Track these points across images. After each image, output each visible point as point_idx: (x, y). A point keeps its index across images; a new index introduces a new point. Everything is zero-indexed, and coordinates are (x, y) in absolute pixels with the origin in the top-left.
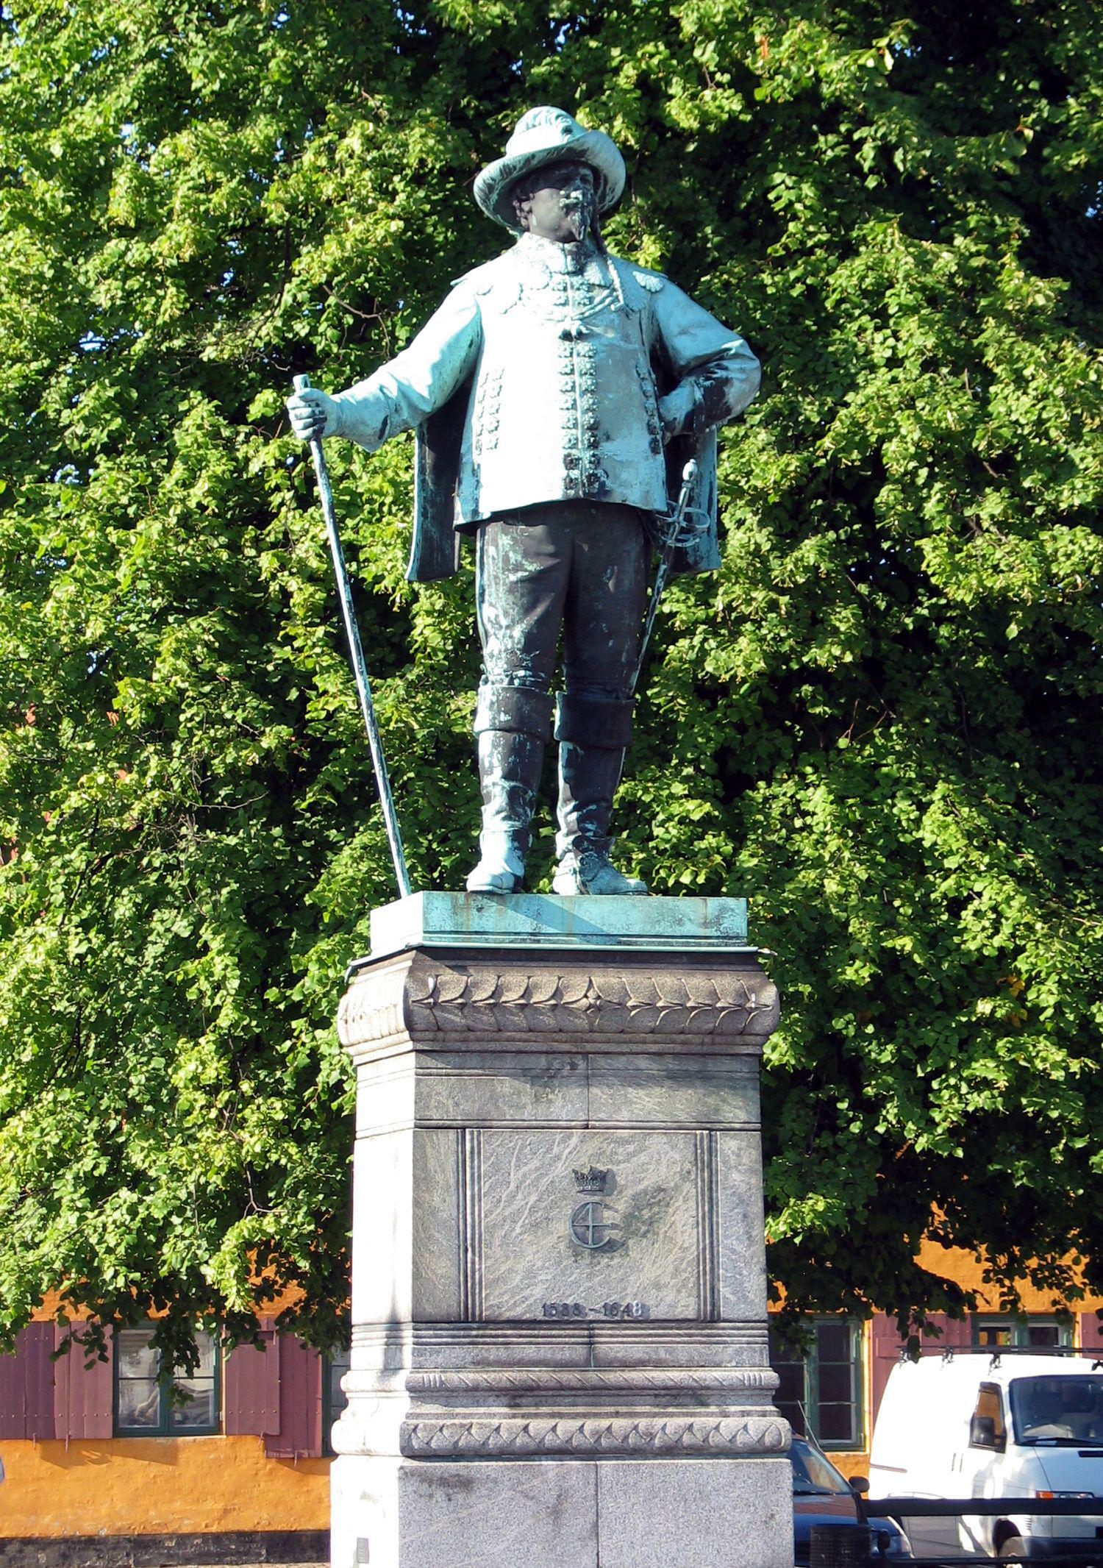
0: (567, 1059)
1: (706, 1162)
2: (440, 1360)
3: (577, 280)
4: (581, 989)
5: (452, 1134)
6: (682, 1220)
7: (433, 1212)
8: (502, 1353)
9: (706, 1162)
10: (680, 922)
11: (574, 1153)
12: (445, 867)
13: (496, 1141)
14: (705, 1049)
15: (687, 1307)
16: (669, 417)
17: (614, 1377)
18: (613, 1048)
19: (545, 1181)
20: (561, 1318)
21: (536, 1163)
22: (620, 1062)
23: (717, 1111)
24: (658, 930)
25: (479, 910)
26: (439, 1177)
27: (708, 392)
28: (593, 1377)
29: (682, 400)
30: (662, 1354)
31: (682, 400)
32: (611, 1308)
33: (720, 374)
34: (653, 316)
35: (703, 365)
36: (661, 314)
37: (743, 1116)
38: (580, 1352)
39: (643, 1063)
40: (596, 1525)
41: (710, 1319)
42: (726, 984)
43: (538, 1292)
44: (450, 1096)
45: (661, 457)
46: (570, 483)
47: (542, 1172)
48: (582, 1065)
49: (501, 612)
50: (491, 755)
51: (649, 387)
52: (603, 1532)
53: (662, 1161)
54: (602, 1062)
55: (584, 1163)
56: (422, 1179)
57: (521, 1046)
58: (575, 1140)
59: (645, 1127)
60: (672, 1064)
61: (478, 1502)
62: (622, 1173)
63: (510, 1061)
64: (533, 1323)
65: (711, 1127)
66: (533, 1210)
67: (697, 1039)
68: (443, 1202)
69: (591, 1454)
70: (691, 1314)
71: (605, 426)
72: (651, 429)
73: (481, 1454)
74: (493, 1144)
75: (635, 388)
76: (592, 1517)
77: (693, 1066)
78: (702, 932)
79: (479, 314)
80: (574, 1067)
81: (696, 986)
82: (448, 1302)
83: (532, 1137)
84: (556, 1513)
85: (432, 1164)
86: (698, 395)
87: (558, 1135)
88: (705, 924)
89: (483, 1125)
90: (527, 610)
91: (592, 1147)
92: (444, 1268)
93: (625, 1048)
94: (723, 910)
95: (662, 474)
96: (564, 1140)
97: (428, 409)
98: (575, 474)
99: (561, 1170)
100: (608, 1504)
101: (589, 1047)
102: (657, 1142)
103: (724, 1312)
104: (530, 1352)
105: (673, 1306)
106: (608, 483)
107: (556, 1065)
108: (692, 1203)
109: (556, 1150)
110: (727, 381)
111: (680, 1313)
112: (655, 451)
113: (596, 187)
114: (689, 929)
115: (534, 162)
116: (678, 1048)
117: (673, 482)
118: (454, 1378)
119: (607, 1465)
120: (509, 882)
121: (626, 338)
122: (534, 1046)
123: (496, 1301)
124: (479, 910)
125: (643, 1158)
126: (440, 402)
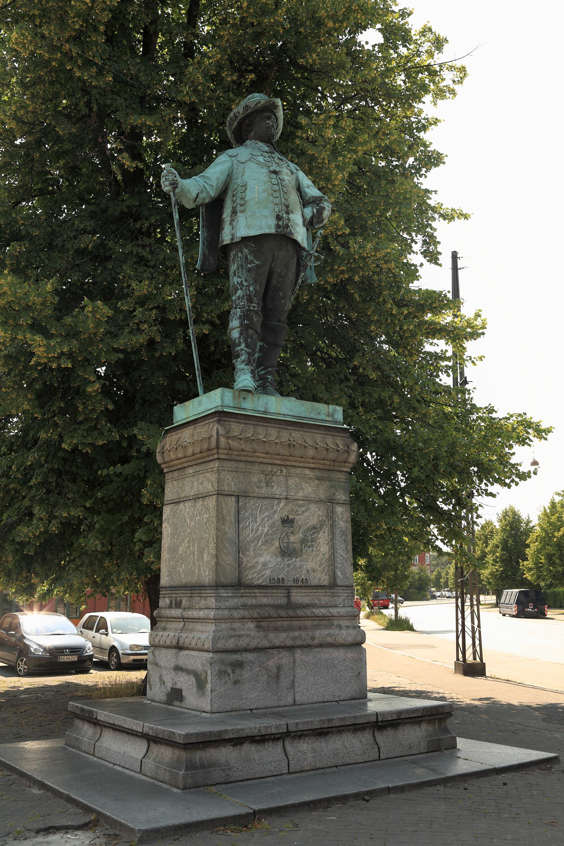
0: (279, 467)
1: (331, 515)
2: (228, 604)
5: (233, 499)
7: (226, 533)
8: (254, 601)
9: (331, 515)
11: (281, 510)
14: (331, 468)
15: (325, 580)
17: (300, 612)
18: (297, 464)
20: (275, 585)
21: (267, 514)
22: (299, 471)
23: (334, 495)
24: (313, 416)
25: (244, 399)
26: (228, 518)
27: (317, 210)
28: (291, 613)
30: (316, 602)
32: (296, 580)
37: (344, 498)
38: (284, 601)
39: (307, 472)
40: (293, 682)
41: (333, 585)
43: (268, 572)
44: (233, 481)
46: (278, 226)
47: (269, 517)
48: (285, 471)
49: (243, 279)
50: (239, 338)
52: (297, 684)
53: (312, 515)
54: (292, 470)
55: (284, 514)
57: (262, 460)
58: (282, 504)
59: (308, 500)
60: (318, 473)
61: (246, 674)
62: (300, 519)
63: (257, 468)
64: (266, 587)
65: (331, 501)
66: (267, 534)
67: (328, 463)
68: (229, 530)
69: (291, 648)
70: (326, 583)
73: (247, 650)
76: (292, 678)
77: (326, 475)
78: (328, 419)
80: (282, 471)
82: (230, 576)
83: (266, 502)
84: (278, 676)
85: (225, 512)
88: (328, 416)
90: (255, 280)
91: (289, 508)
92: (229, 560)
93: (301, 465)
94: (335, 410)
96: (278, 504)
98: (281, 223)
99: (277, 517)
100: (300, 673)
101: (288, 463)
103: (339, 582)
104: (265, 601)
105: (320, 580)
107: (275, 470)
108: (326, 534)
109: (275, 508)
115: (259, 105)
116: (321, 467)
118: (236, 614)
119: (298, 652)
122: (266, 461)
123: (252, 576)
124: (244, 399)
125: (307, 514)
126: (216, 195)
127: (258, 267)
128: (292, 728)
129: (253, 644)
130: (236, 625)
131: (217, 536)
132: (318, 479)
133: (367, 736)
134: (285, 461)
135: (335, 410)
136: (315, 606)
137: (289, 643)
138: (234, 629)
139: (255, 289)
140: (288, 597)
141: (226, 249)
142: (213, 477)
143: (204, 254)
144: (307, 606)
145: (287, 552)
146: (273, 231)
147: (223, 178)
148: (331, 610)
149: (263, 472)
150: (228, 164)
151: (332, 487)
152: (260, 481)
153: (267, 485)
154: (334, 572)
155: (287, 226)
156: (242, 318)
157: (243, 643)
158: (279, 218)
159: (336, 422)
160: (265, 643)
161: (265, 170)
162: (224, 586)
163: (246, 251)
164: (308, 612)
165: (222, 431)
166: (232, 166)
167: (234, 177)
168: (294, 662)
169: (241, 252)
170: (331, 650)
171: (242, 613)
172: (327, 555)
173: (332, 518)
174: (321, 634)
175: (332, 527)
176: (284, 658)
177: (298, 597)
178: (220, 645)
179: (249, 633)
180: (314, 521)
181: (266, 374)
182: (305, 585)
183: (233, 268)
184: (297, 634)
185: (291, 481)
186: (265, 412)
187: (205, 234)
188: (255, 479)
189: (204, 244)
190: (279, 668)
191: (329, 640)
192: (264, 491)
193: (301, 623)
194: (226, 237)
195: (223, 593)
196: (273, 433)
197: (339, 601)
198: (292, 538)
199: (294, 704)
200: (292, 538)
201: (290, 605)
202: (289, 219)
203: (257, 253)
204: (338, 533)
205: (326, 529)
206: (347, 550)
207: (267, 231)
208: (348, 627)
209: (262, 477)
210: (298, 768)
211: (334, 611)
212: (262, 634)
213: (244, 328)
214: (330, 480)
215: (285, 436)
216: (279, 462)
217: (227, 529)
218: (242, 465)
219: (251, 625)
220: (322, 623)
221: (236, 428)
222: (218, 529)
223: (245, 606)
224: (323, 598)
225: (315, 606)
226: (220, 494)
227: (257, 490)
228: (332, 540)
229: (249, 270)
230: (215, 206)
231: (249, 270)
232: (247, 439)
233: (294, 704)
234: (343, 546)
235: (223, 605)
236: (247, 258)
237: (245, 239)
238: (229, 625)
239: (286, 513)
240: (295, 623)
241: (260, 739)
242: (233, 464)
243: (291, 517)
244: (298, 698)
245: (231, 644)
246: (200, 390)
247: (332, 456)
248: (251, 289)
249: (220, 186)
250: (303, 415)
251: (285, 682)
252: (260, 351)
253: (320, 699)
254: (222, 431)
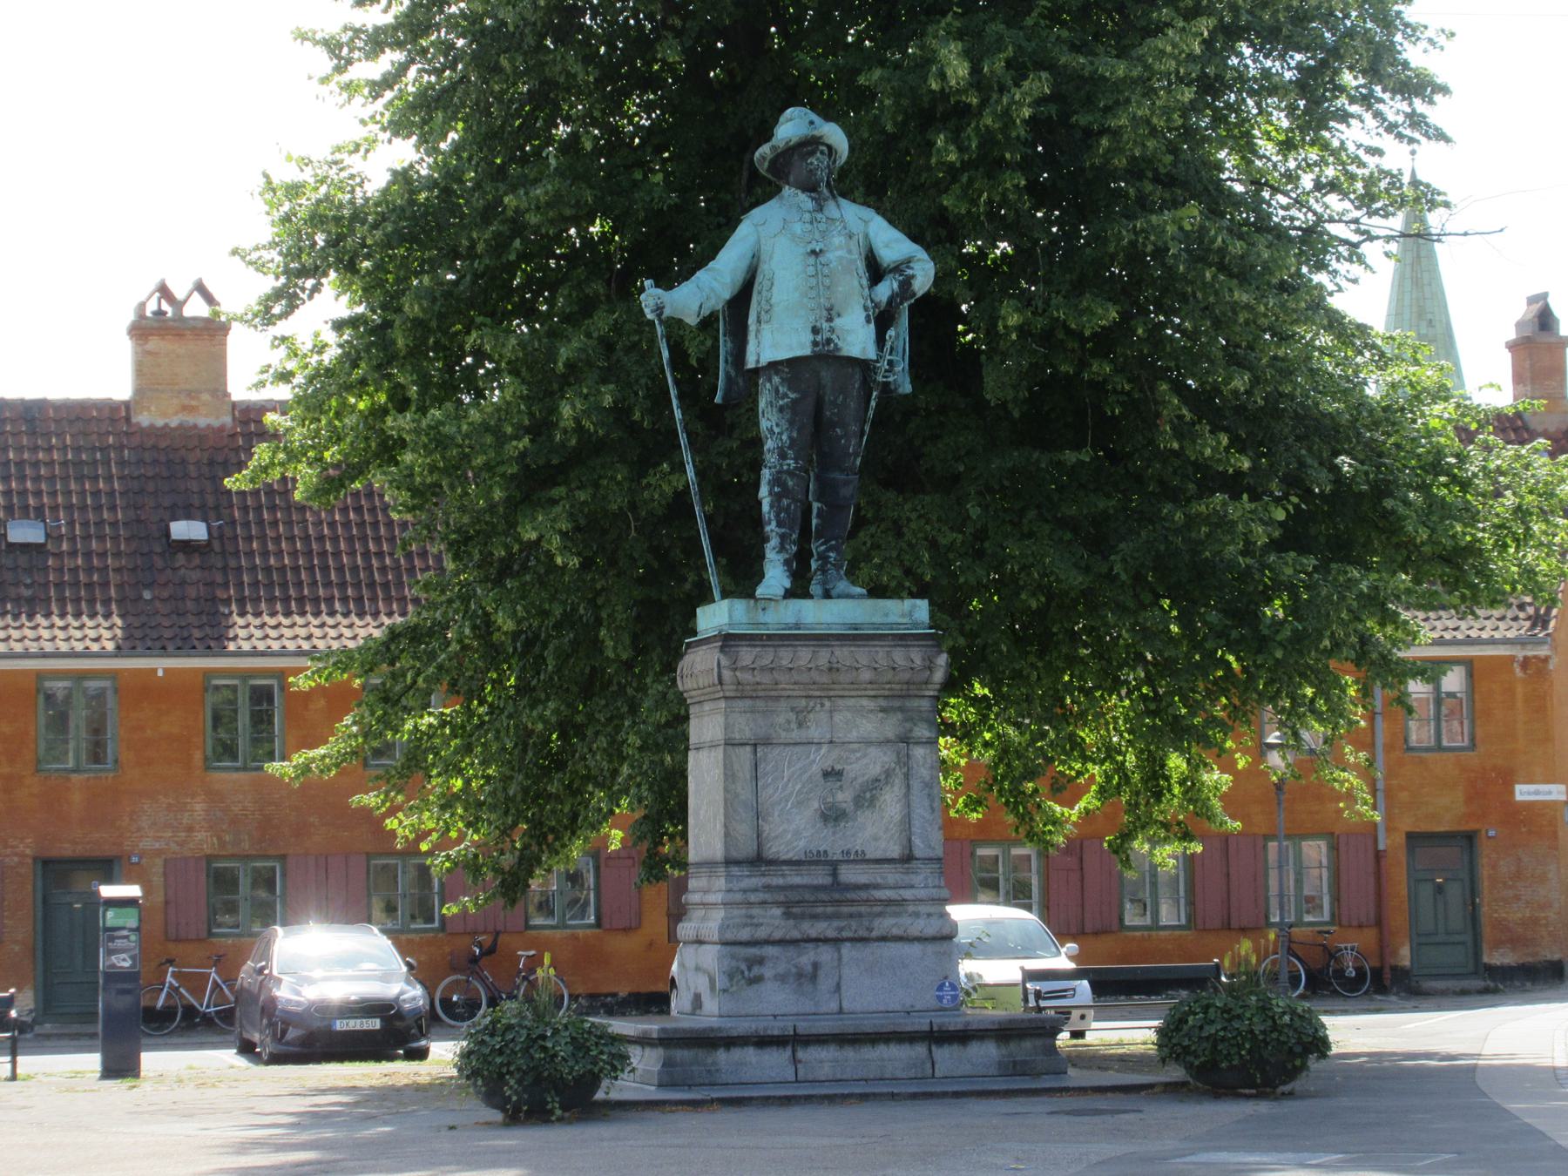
1: (905, 761)
3: (819, 216)
5: (748, 748)
7: (737, 795)
8: (781, 881)
10: (887, 615)
11: (822, 758)
12: (743, 579)
13: (777, 751)
15: (895, 851)
16: (877, 299)
17: (849, 896)
19: (805, 777)
21: (799, 765)
22: (851, 702)
23: (911, 731)
24: (875, 620)
28: (837, 896)
29: (884, 290)
30: (879, 881)
31: (884, 290)
33: (909, 272)
34: (866, 236)
35: (897, 269)
36: (872, 235)
38: (828, 880)
39: (865, 702)
41: (908, 858)
42: (917, 656)
43: (802, 844)
45: (872, 326)
46: (815, 344)
48: (827, 704)
51: (865, 282)
52: (843, 988)
53: (875, 762)
54: (840, 702)
55: (827, 765)
56: (729, 775)
58: (823, 751)
60: (883, 703)
61: (768, 971)
63: (783, 704)
64: (798, 863)
68: (745, 793)
69: (836, 941)
71: (836, 308)
72: (866, 308)
73: (768, 942)
74: (774, 753)
75: (856, 283)
77: (897, 703)
79: (758, 242)
80: (822, 705)
82: (747, 849)
84: (814, 977)
85: (736, 767)
86: (895, 285)
87: (814, 748)
88: (903, 616)
89: (767, 742)
90: (791, 423)
91: (835, 753)
92: (744, 830)
95: (873, 336)
96: (818, 750)
97: (727, 295)
98: (819, 338)
99: (816, 769)
100: (846, 972)
102: (873, 751)
103: (917, 853)
104: (797, 880)
106: (840, 344)
110: (913, 276)
111: (889, 855)
112: (868, 321)
113: (830, 155)
114: (893, 619)
117: (880, 340)
118: (753, 898)
119: (847, 950)
120: (782, 592)
121: (850, 252)
123: (775, 849)
125: (865, 761)
127: (794, 402)
128: (800, 1031)
129: (778, 935)
130: (755, 911)
131: (726, 800)
132: (883, 710)
133: (920, 1050)
134: (827, 690)
135: (914, 606)
136: (877, 887)
137: (831, 934)
138: (751, 917)
139: (790, 437)
140: (834, 874)
141: (756, 371)
142: (720, 719)
143: (727, 374)
144: (866, 887)
145: (832, 816)
146: (807, 351)
147: (743, 265)
148: (902, 892)
149: (793, 709)
150: (752, 239)
151: (906, 720)
152: (789, 722)
153: (800, 725)
154: (910, 840)
155: (829, 341)
156: (772, 483)
157: (761, 933)
158: (815, 331)
159: (916, 625)
160: (796, 934)
161: (802, 250)
162: (737, 863)
163: (776, 379)
164: (863, 895)
165: (724, 662)
166: (758, 242)
167: (763, 257)
168: (840, 959)
169: (770, 380)
170: (899, 945)
171: (761, 896)
172: (898, 817)
173: (906, 764)
175: (907, 776)
176: (825, 954)
177: (849, 875)
178: (729, 936)
179: (773, 922)
180: (875, 770)
181: (828, 550)
182: (862, 860)
183: (762, 404)
184: (843, 924)
185: (838, 717)
186: (797, 626)
187: (729, 345)
188: (781, 719)
189: (726, 361)
190: (816, 966)
191: (895, 931)
192: (796, 735)
193: (853, 909)
194: (751, 363)
195: (735, 870)
196: (804, 655)
197: (917, 880)
198: (840, 796)
199: (841, 1011)
200: (840, 796)
201: (837, 885)
202: (832, 330)
203: (791, 383)
204: (916, 785)
205: (898, 781)
206: (933, 810)
207: (799, 353)
208: (929, 915)
209: (792, 716)
210: (810, 1077)
211: (907, 894)
212: (791, 922)
213: (776, 498)
214: (901, 709)
215: (824, 657)
216: (818, 693)
217: (739, 789)
218: (760, 704)
219: (777, 911)
220: (888, 909)
221: (747, 655)
222: (726, 790)
223: (768, 888)
224: (891, 875)
225: (877, 887)
226: (729, 743)
227: (783, 734)
228: (907, 794)
229: (781, 409)
230: (740, 302)
231: (781, 409)
232: (763, 669)
233: (841, 1011)
234: (926, 803)
235: (736, 885)
236: (777, 391)
237: (774, 366)
238: (743, 911)
239: (829, 763)
240: (845, 909)
241: (763, 1042)
242: (748, 703)
243: (838, 767)
244: (845, 1005)
245: (745, 935)
246: (716, 594)
247: (906, 676)
248: (784, 437)
249: (739, 277)
250: (859, 620)
251: (825, 984)
252: (818, 516)
253: (882, 1008)
254: (724, 662)
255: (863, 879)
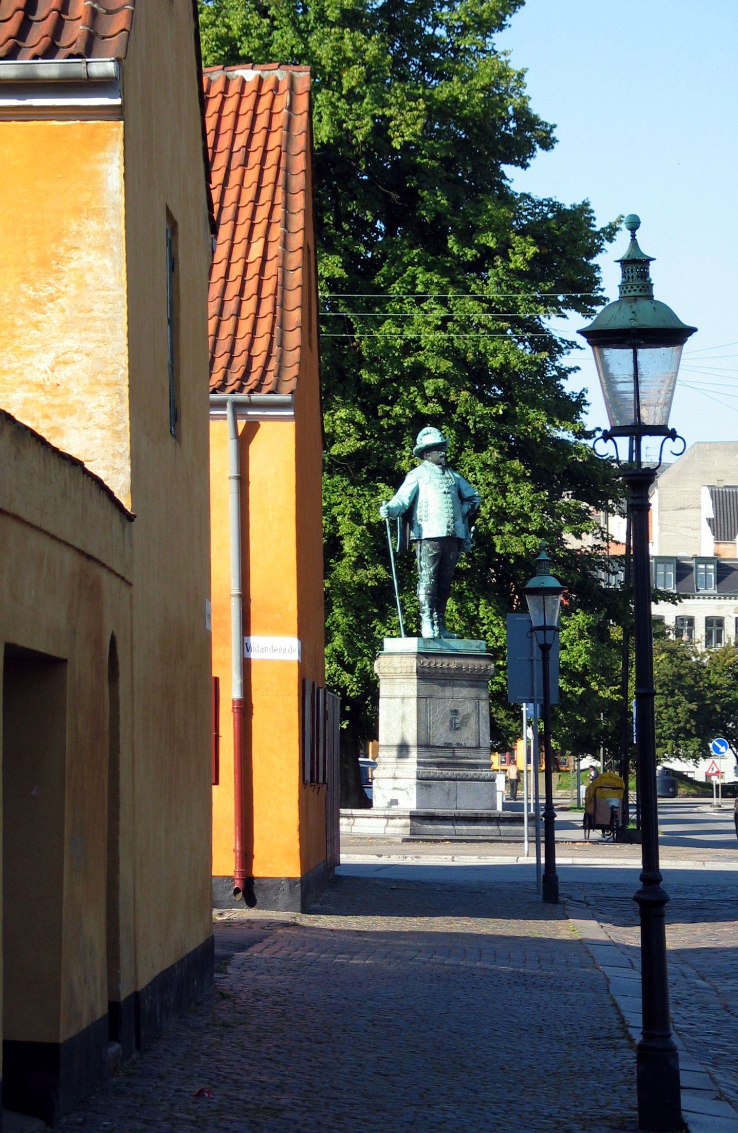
1: (477, 707)
4: (454, 663)
6: (473, 721)
9: (477, 707)
15: (474, 744)
20: (448, 746)
28: (455, 761)
32: (458, 744)
38: (451, 755)
39: (464, 682)
41: (478, 747)
42: (483, 663)
46: (448, 532)
63: (437, 681)
64: (442, 747)
77: (474, 683)
81: (471, 663)
82: (424, 742)
83: (441, 701)
84: (448, 794)
89: (430, 697)
90: (434, 564)
92: (423, 733)
100: (459, 792)
104: (441, 754)
123: (433, 742)
174: (471, 773)
224: (472, 753)
255: (463, 755)
